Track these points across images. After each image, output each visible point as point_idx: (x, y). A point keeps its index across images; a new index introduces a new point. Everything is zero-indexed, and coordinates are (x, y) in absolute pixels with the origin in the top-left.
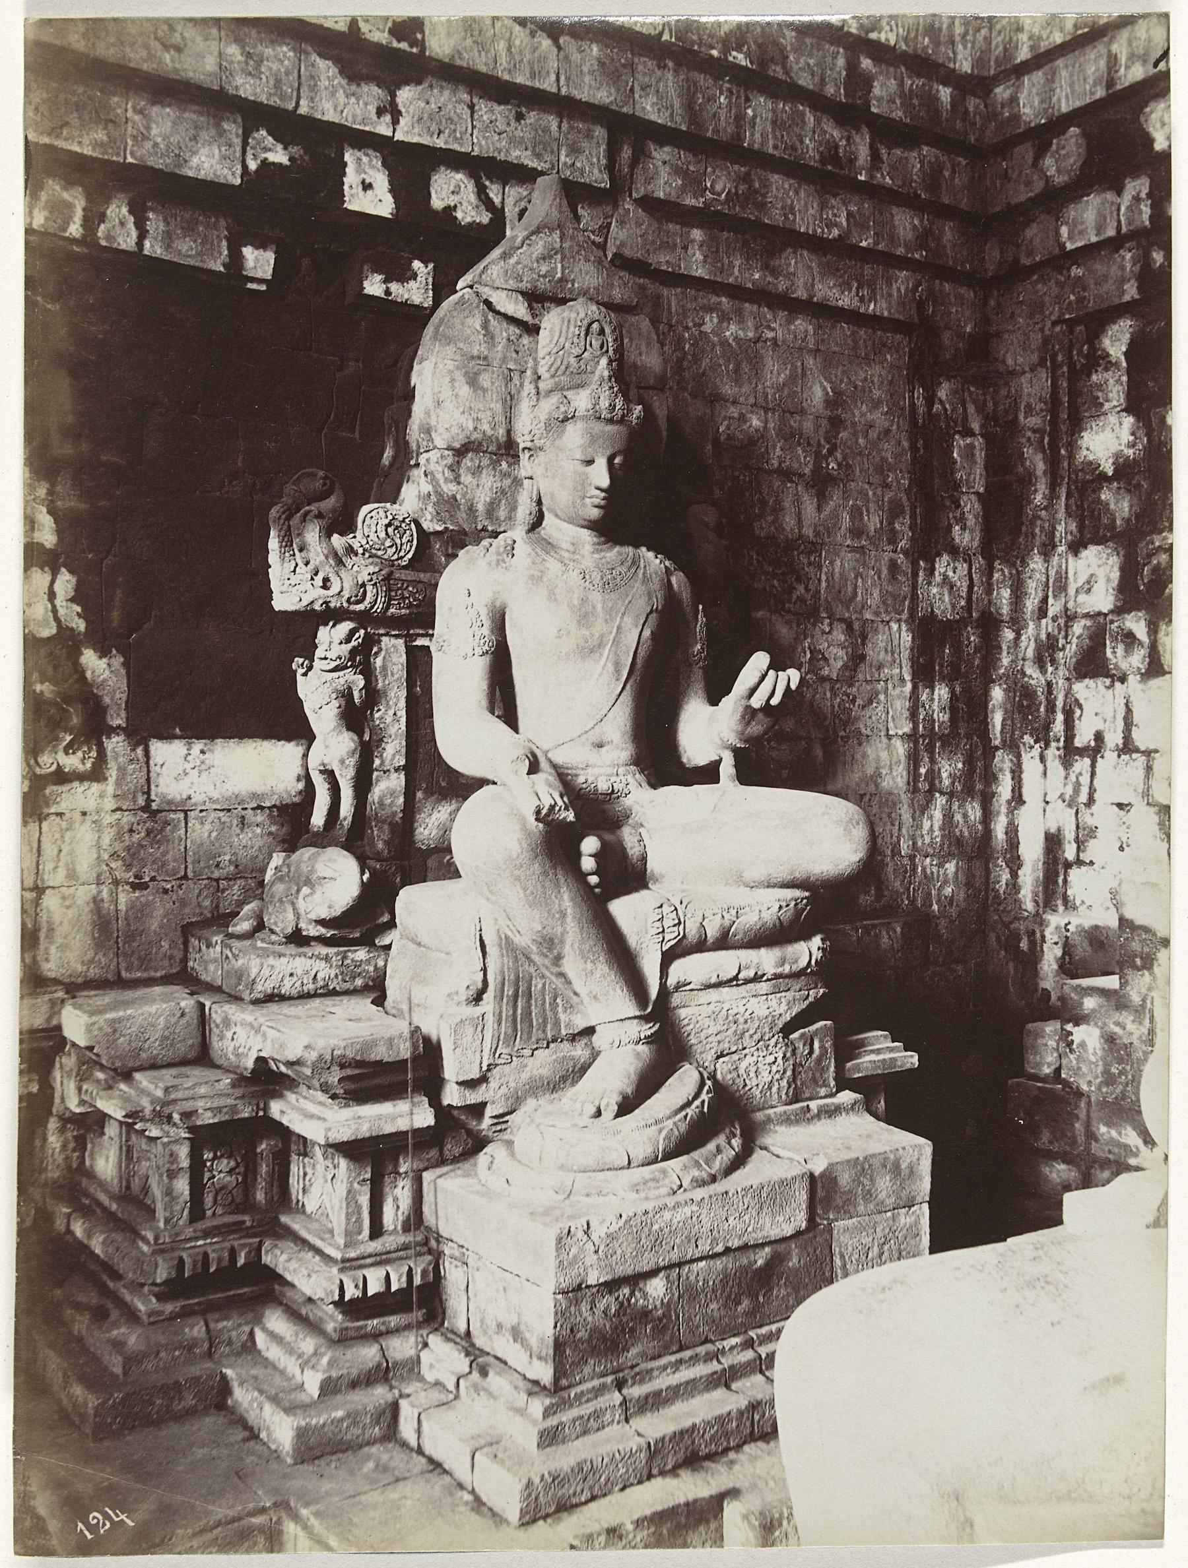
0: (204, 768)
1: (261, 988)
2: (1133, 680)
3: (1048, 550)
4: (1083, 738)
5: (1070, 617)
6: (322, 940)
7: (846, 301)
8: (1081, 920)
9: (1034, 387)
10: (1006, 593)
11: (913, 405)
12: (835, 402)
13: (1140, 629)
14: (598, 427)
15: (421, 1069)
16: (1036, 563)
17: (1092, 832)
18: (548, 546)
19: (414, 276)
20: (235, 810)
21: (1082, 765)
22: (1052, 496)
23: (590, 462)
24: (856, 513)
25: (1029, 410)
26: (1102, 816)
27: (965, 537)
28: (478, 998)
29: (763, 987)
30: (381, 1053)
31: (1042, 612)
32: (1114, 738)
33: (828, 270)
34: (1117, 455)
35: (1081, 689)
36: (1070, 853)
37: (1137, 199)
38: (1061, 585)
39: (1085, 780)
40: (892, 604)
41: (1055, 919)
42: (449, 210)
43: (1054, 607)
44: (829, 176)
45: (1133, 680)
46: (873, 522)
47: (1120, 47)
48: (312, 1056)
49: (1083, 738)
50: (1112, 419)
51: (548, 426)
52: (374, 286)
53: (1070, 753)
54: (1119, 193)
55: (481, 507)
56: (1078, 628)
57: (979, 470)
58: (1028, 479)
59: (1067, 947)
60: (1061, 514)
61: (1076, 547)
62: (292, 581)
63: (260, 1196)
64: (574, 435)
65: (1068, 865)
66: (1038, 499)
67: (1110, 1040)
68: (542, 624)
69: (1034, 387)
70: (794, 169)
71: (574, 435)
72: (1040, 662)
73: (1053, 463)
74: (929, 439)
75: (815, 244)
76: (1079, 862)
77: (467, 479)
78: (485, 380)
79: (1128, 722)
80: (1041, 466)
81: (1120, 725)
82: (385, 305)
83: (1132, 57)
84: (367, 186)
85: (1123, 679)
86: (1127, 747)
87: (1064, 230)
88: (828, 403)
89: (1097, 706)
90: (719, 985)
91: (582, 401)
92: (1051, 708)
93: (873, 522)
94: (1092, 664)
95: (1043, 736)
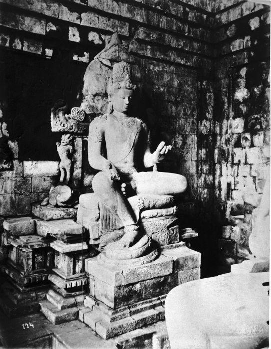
0: (36, 167)
1: (49, 217)
2: (247, 148)
3: (228, 119)
4: (236, 161)
5: (233, 134)
6: (62, 207)
7: (182, 62)
8: (235, 203)
9: (225, 82)
12: (180, 85)
14: (126, 90)
15: (84, 236)
16: (225, 122)
17: (238, 183)
18: (115, 117)
19: (85, 56)
20: (43, 177)
21: (235, 167)
22: (229, 107)
23: (124, 98)
24: (184, 110)
25: (224, 88)
26: (240, 179)
28: (98, 220)
29: (163, 218)
30: (76, 232)
31: (226, 133)
32: (243, 161)
33: (178, 55)
34: (243, 98)
36: (233, 187)
37: (247, 41)
38: (231, 127)
39: (236, 170)
40: (193, 130)
41: (229, 202)
42: (93, 41)
43: (229, 132)
44: (179, 35)
45: (247, 148)
46: (189, 112)
48: (60, 233)
49: (236, 161)
50: (242, 89)
51: (115, 90)
52: (75, 58)
53: (233, 164)
54: (244, 39)
55: (99, 108)
57: (212, 101)
58: (224, 103)
59: (232, 209)
60: (231, 111)
61: (234, 118)
62: (56, 125)
63: (48, 265)
64: (121, 92)
65: (232, 190)
66: (226, 107)
67: (242, 230)
68: (114, 133)
69: (225, 82)
70: (171, 32)
71: (121, 92)
72: (226, 144)
74: (201, 93)
75: (175, 49)
76: (235, 189)
77: (96, 101)
78: (100, 79)
79: (246, 158)
80: (226, 100)
81: (244, 158)
82: (78, 62)
83: (246, 9)
84: (74, 35)
85: (245, 148)
86: (246, 163)
87: (231, 47)
88: (178, 85)
89: (239, 154)
90: (152, 217)
91: (122, 84)
92: (229, 154)
93: (189, 112)
94: (238, 144)
95: (227, 161)
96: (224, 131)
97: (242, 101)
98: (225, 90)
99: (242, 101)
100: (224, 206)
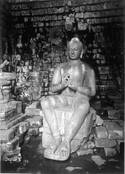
2: (22, 66)
3: (14, 54)
4: (18, 71)
5: (16, 61)
9: (12, 40)
10: (10, 58)
11: (2, 39)
13: (23, 62)
16: (13, 55)
17: (19, 79)
21: (18, 74)
22: (14, 50)
25: (12, 42)
26: (20, 78)
27: (6, 52)
29: (8, 90)
31: (14, 60)
32: (21, 71)
34: (20, 47)
35: (17, 67)
36: (17, 81)
38: (15, 58)
43: (15, 60)
45: (22, 66)
47: (22, 12)
49: (18, 71)
56: (17, 62)
58: (12, 48)
59: (17, 89)
61: (17, 54)
65: (17, 82)
66: (13, 50)
69: (12, 40)
72: (14, 64)
73: (14, 47)
76: (17, 82)
85: (21, 66)
86: (22, 72)
87: (16, 26)
89: (19, 69)
94: (18, 65)
95: (14, 71)
96: (13, 59)
97: (20, 48)
98: (12, 42)
99: (20, 48)
100: (13, 89)
